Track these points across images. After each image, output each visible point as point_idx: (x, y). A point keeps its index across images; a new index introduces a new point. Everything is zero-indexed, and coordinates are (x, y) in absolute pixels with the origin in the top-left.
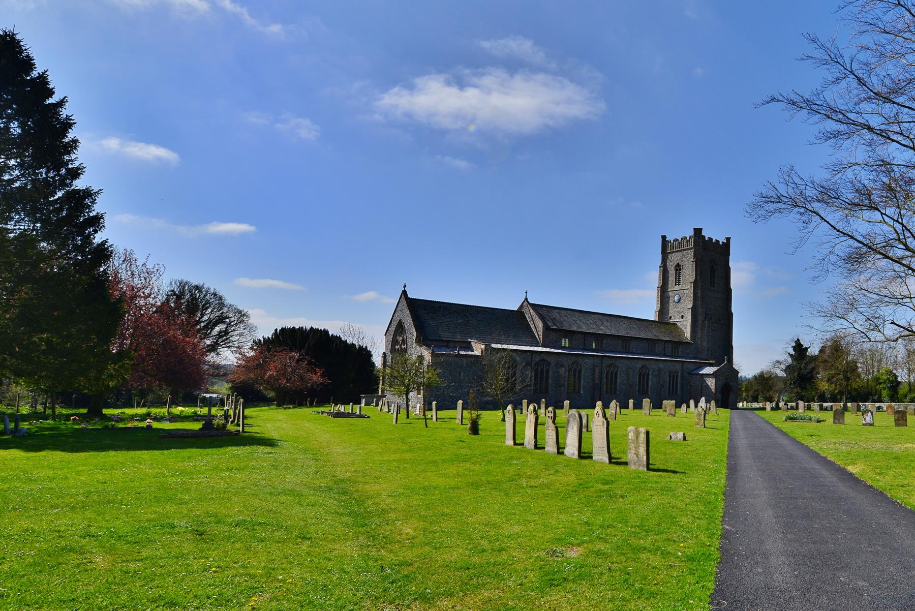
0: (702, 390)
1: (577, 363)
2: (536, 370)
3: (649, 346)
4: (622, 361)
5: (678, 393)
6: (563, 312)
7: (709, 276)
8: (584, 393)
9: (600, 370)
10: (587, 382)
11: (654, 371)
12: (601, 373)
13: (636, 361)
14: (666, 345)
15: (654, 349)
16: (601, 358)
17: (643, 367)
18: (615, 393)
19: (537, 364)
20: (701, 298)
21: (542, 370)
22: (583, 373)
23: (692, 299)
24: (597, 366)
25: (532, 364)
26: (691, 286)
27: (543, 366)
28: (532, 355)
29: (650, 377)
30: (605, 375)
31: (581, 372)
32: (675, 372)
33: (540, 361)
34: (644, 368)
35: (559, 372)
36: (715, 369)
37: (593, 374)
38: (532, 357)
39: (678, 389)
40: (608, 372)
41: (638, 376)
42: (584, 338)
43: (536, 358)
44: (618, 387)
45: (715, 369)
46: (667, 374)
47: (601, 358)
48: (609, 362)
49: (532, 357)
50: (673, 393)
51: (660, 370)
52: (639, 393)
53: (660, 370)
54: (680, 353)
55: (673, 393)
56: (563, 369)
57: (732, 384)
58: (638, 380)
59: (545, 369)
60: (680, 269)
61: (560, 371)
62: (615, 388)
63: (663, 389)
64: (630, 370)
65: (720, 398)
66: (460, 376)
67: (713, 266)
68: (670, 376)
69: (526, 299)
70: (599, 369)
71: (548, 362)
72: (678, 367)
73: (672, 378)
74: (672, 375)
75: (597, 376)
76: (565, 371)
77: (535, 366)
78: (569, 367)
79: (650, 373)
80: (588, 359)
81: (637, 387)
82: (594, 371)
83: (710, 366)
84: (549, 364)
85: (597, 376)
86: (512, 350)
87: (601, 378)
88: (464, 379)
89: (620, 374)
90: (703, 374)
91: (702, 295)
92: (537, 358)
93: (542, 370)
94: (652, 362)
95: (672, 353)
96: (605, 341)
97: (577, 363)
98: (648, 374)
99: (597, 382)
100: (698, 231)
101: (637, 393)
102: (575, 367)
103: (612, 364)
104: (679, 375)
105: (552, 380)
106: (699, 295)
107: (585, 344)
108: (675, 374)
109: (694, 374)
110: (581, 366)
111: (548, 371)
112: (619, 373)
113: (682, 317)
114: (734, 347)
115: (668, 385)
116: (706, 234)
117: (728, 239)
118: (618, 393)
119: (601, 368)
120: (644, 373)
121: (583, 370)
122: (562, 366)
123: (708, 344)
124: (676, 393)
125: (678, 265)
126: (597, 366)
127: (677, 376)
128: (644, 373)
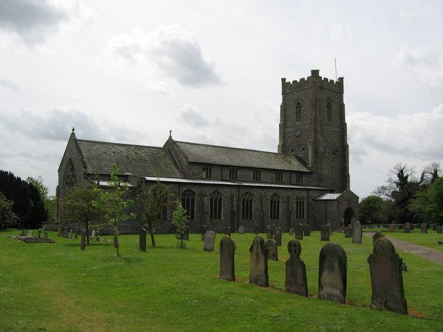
4: (256, 190)
12: (238, 200)
17: (274, 195)
18: (251, 218)
19: (184, 194)
36: (338, 195)
37: (233, 201)
44: (253, 214)
45: (338, 195)
48: (245, 191)
50: (300, 218)
52: (271, 218)
55: (300, 218)
62: (251, 213)
68: (297, 203)
69: (170, 137)
71: (194, 192)
72: (304, 194)
82: (233, 198)
84: (194, 193)
86: (162, 182)
87: (238, 206)
90: (326, 200)
92: (185, 189)
94: (281, 191)
96: (239, 173)
98: (278, 202)
104: (305, 201)
111: (193, 200)
117: (341, 79)
118: (253, 218)
121: (223, 199)
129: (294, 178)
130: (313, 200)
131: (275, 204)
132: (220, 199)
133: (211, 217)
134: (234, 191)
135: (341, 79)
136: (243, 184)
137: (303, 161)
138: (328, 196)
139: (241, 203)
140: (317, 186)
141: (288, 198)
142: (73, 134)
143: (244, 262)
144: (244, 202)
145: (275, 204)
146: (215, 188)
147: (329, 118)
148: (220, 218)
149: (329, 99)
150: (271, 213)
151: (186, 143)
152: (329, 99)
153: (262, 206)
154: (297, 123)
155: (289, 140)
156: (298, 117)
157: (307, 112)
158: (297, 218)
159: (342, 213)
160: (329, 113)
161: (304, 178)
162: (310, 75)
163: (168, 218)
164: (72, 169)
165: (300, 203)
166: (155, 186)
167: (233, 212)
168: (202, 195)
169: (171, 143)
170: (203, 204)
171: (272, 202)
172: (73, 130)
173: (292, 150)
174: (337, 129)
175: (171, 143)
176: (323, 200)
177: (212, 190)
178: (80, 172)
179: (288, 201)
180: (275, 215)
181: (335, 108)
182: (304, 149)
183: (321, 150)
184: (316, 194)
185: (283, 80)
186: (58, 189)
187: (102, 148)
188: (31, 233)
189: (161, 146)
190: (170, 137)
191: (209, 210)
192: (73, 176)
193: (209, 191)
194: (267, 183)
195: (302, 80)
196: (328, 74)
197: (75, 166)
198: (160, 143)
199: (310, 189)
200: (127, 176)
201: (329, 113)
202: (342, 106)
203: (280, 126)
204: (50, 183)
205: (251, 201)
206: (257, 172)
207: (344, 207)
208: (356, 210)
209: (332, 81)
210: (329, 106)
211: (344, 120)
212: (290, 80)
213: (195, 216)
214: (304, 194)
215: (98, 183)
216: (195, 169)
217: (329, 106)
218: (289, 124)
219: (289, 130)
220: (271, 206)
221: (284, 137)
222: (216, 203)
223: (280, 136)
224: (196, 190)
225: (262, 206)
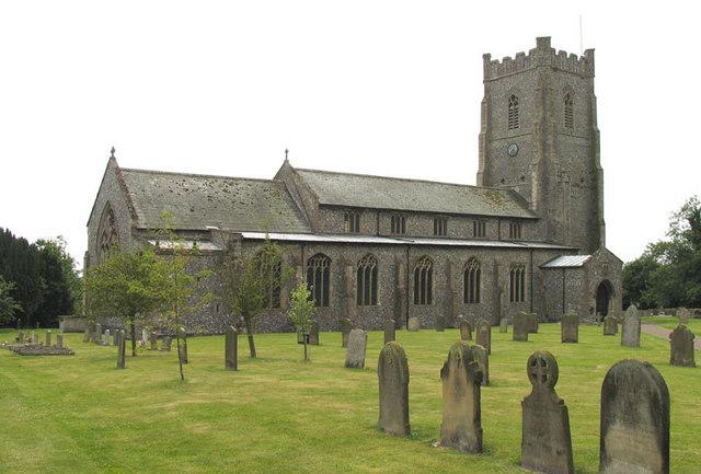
5: (526, 299)
6: (341, 178)
12: (407, 272)
17: (470, 260)
18: (430, 303)
19: (311, 262)
21: (318, 271)
22: (379, 273)
29: (482, 276)
36: (585, 258)
37: (397, 274)
39: (526, 292)
42: (378, 219)
44: (434, 293)
48: (420, 254)
68: (512, 273)
69: (286, 161)
72: (524, 258)
82: (397, 268)
84: (329, 260)
86: (273, 241)
90: (564, 268)
92: (311, 252)
93: (318, 271)
95: (511, 236)
98: (479, 272)
102: (368, 264)
109: (550, 268)
111: (327, 272)
115: (509, 286)
118: (434, 302)
121: (380, 268)
124: (522, 300)
127: (523, 273)
129: (506, 228)
130: (541, 268)
131: (472, 277)
133: (359, 303)
134: (400, 254)
135: (590, 52)
136: (417, 242)
137: (521, 200)
138: (567, 261)
139: (412, 276)
140: (545, 243)
141: (496, 265)
142: (113, 158)
143: (426, 382)
144: (417, 275)
145: (472, 277)
146: (366, 251)
147: (569, 122)
149: (567, 87)
150: (466, 293)
151: (314, 171)
152: (567, 87)
154: (512, 133)
155: (497, 163)
157: (529, 111)
158: (512, 300)
159: (593, 289)
160: (569, 112)
162: (534, 45)
163: (283, 306)
164: (112, 220)
165: (517, 274)
166: (259, 248)
167: (398, 294)
168: (343, 263)
169: (287, 173)
170: (345, 280)
172: (113, 151)
173: (503, 181)
174: (583, 142)
175: (287, 173)
176: (555, 268)
177: (357, 255)
178: (125, 225)
180: (472, 296)
181: (579, 104)
182: (523, 178)
183: (554, 179)
184: (545, 257)
185: (487, 57)
186: (88, 257)
187: (166, 183)
188: (38, 336)
189: (271, 176)
190: (286, 161)
191: (355, 289)
192: (114, 232)
193: (354, 256)
194: (458, 239)
195: (521, 55)
196: (568, 43)
197: (117, 215)
198: (269, 173)
199: (533, 249)
200: (210, 231)
201: (569, 112)
203: (481, 137)
204: (77, 248)
205: (430, 272)
206: (440, 220)
207: (596, 279)
208: (617, 283)
209: (574, 56)
210: (568, 101)
212: (497, 56)
213: (330, 301)
214: (524, 258)
215: (157, 244)
216: (332, 217)
217: (568, 101)
218: (496, 134)
219: (496, 144)
220: (466, 280)
221: (487, 157)
222: (368, 277)
223: (480, 156)
224: (330, 253)
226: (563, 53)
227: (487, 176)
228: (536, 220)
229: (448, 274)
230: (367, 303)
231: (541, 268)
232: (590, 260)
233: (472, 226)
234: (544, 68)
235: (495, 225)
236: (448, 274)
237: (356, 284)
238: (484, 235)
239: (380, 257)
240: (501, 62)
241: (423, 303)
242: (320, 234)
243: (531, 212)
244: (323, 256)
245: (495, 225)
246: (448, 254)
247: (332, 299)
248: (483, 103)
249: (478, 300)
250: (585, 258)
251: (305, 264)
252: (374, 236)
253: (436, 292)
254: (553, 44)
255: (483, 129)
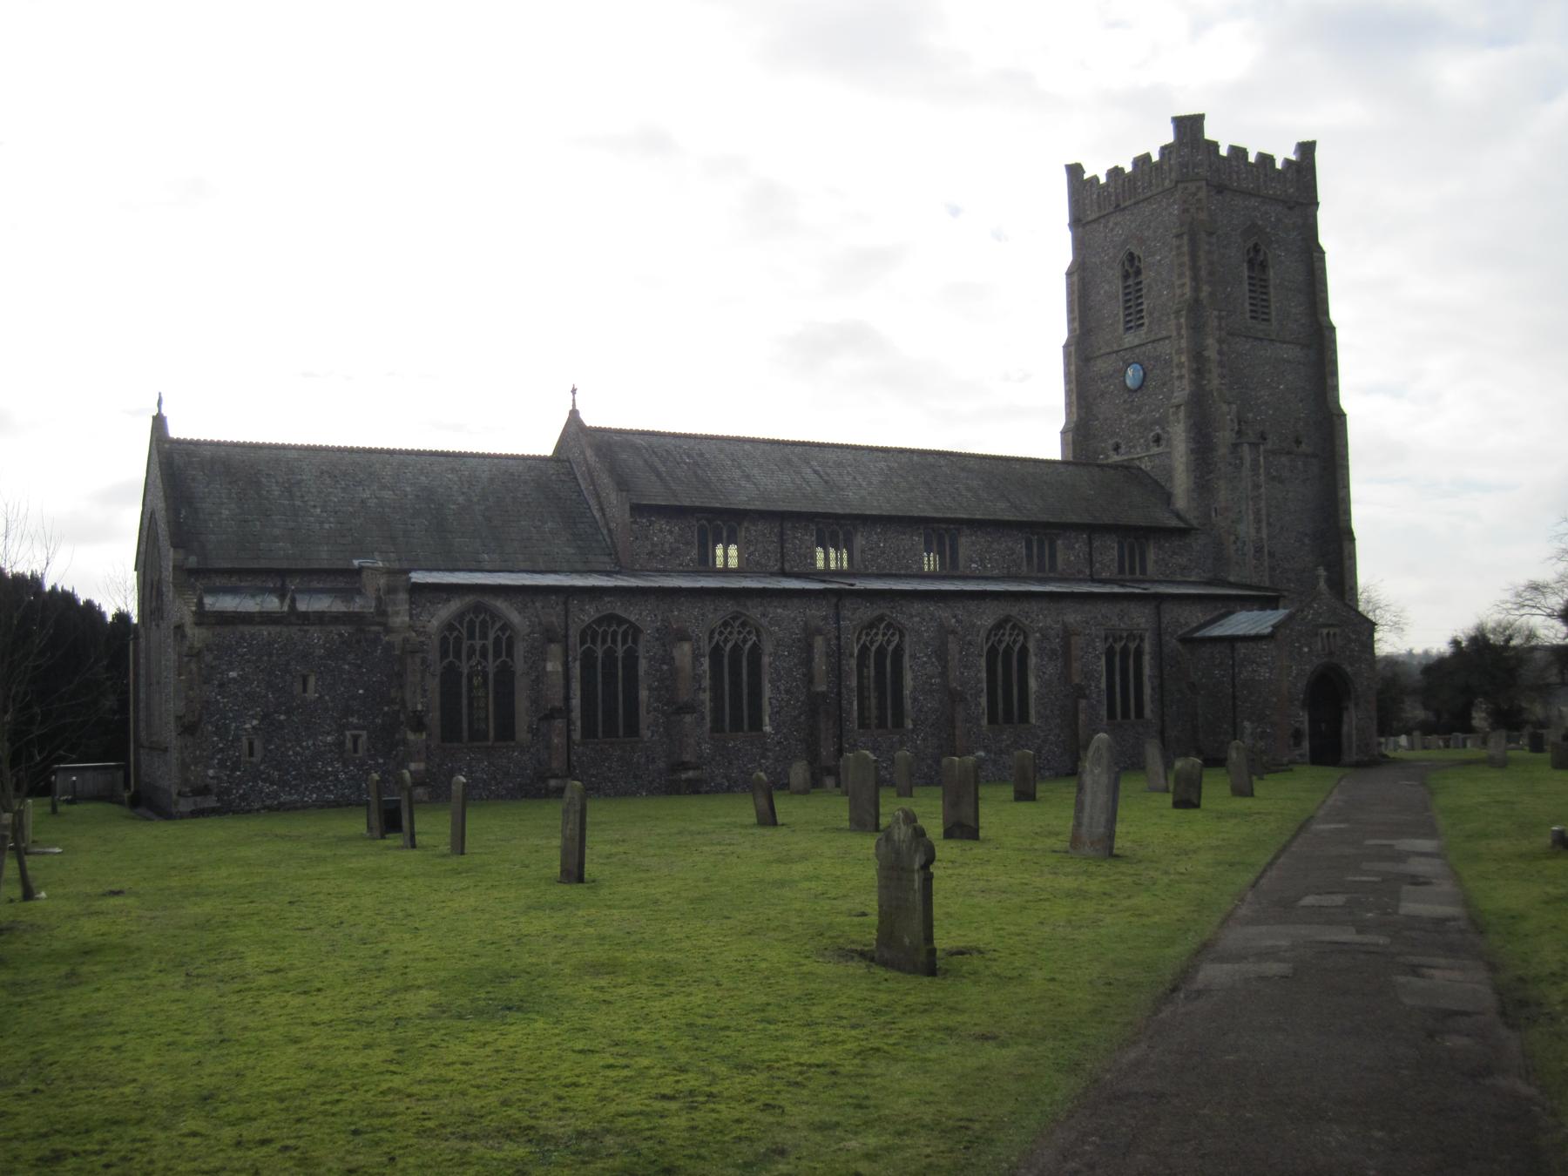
0: (1234, 697)
1: (743, 624)
2: (588, 661)
3: (1029, 547)
4: (917, 607)
7: (1246, 287)
8: (777, 729)
9: (834, 642)
10: (787, 692)
11: (1045, 637)
12: (837, 655)
13: (972, 605)
14: (1096, 544)
15: (1053, 556)
16: (834, 600)
17: (999, 625)
18: (898, 723)
19: (588, 634)
20: (1221, 364)
21: (610, 655)
22: (766, 660)
23: (1184, 371)
24: (819, 631)
25: (566, 636)
26: (1179, 327)
27: (614, 641)
28: (565, 603)
29: (1033, 661)
30: (853, 662)
31: (759, 657)
32: (1131, 637)
33: (599, 621)
34: (1008, 627)
35: (673, 658)
37: (808, 662)
38: (567, 611)
40: (864, 650)
41: (983, 662)
42: (782, 534)
43: (582, 610)
44: (908, 703)
46: (1100, 646)
47: (834, 600)
48: (867, 612)
49: (567, 611)
50: (1125, 715)
51: (1067, 634)
52: (992, 720)
53: (1067, 634)
54: (1151, 567)
55: (1125, 715)
56: (686, 647)
57: (1349, 669)
58: (984, 675)
59: (620, 651)
60: (1138, 272)
61: (676, 653)
63: (1083, 703)
64: (951, 637)
65: (1306, 725)
66: (305, 690)
67: (1256, 249)
70: (828, 641)
71: (632, 625)
73: (1117, 659)
74: (1118, 647)
75: (820, 664)
76: (696, 657)
77: (583, 642)
78: (711, 638)
79: (1031, 646)
80: (785, 607)
81: (984, 701)
83: (1262, 608)
84: (635, 631)
85: (820, 664)
87: (837, 673)
88: (321, 697)
89: (913, 657)
91: (1220, 352)
92: (589, 613)
93: (610, 655)
95: (1121, 570)
97: (743, 624)
98: (1024, 651)
99: (823, 688)
100: (1189, 127)
101: (985, 722)
103: (881, 618)
104: (1147, 647)
105: (650, 689)
106: (1212, 353)
107: (782, 556)
108: (1132, 646)
110: (758, 632)
111: (631, 659)
112: (906, 658)
113: (1158, 440)
114: (1356, 534)
115: (1103, 685)
116: (1221, 133)
117: (1307, 150)
118: (909, 725)
119: (838, 638)
120: (1008, 652)
121: (768, 647)
122: (683, 636)
123: (1258, 530)
124: (1140, 712)
125: (1131, 257)
126: (819, 631)
127: (1139, 653)
128: (1008, 652)
132: (756, 652)
133: (717, 726)
135: (1307, 150)
144: (862, 664)
146: (730, 607)
147: (1260, 310)
148: (756, 724)
153: (944, 674)
154: (1130, 339)
156: (1134, 316)
160: (1259, 285)
161: (1152, 555)
162: (1169, 137)
163: (522, 734)
165: (1122, 657)
171: (992, 652)
173: (1117, 448)
174: (1290, 352)
177: (715, 615)
179: (1067, 646)
184: (1192, 616)
185: (1075, 171)
191: (706, 696)
195: (1142, 161)
201: (1259, 285)
202: (1313, 260)
205: (898, 653)
209: (1266, 160)
210: (1257, 264)
211: (1326, 313)
212: (1096, 169)
213: (643, 725)
214: (1140, 618)
216: (664, 533)
217: (1257, 264)
219: (1102, 366)
220: (991, 671)
224: (644, 617)
225: (944, 674)
226: (1238, 153)
227: (1079, 432)
228: (1183, 532)
229: (941, 654)
230: (736, 725)
231: (1186, 640)
232: (1290, 617)
233: (1021, 548)
234: (1192, 187)
235: (1080, 545)
236: (941, 654)
237: (706, 683)
238: (1053, 567)
239: (764, 622)
240: (1103, 180)
241: (882, 724)
242: (633, 573)
243: (1178, 516)
244: (620, 621)
245: (1080, 545)
246: (943, 613)
247: (645, 718)
248: (1069, 274)
249: (1024, 717)
250: (1280, 614)
251: (574, 639)
252: (772, 574)
253: (915, 700)
254: (1210, 134)
255: (1071, 331)
